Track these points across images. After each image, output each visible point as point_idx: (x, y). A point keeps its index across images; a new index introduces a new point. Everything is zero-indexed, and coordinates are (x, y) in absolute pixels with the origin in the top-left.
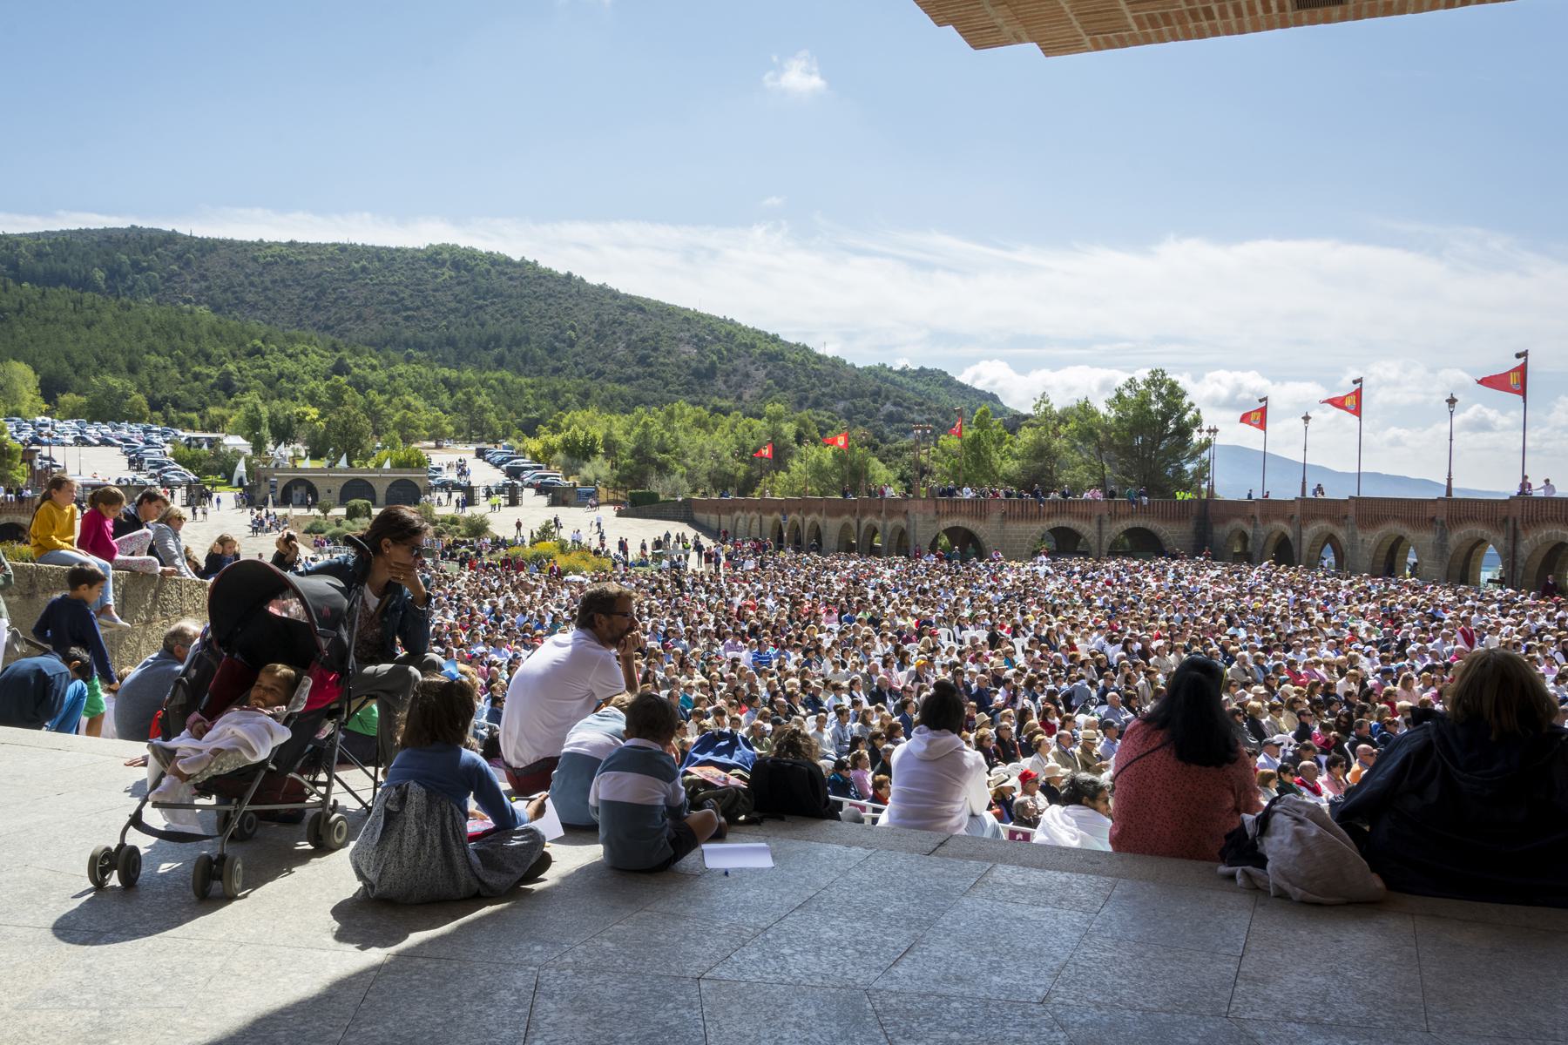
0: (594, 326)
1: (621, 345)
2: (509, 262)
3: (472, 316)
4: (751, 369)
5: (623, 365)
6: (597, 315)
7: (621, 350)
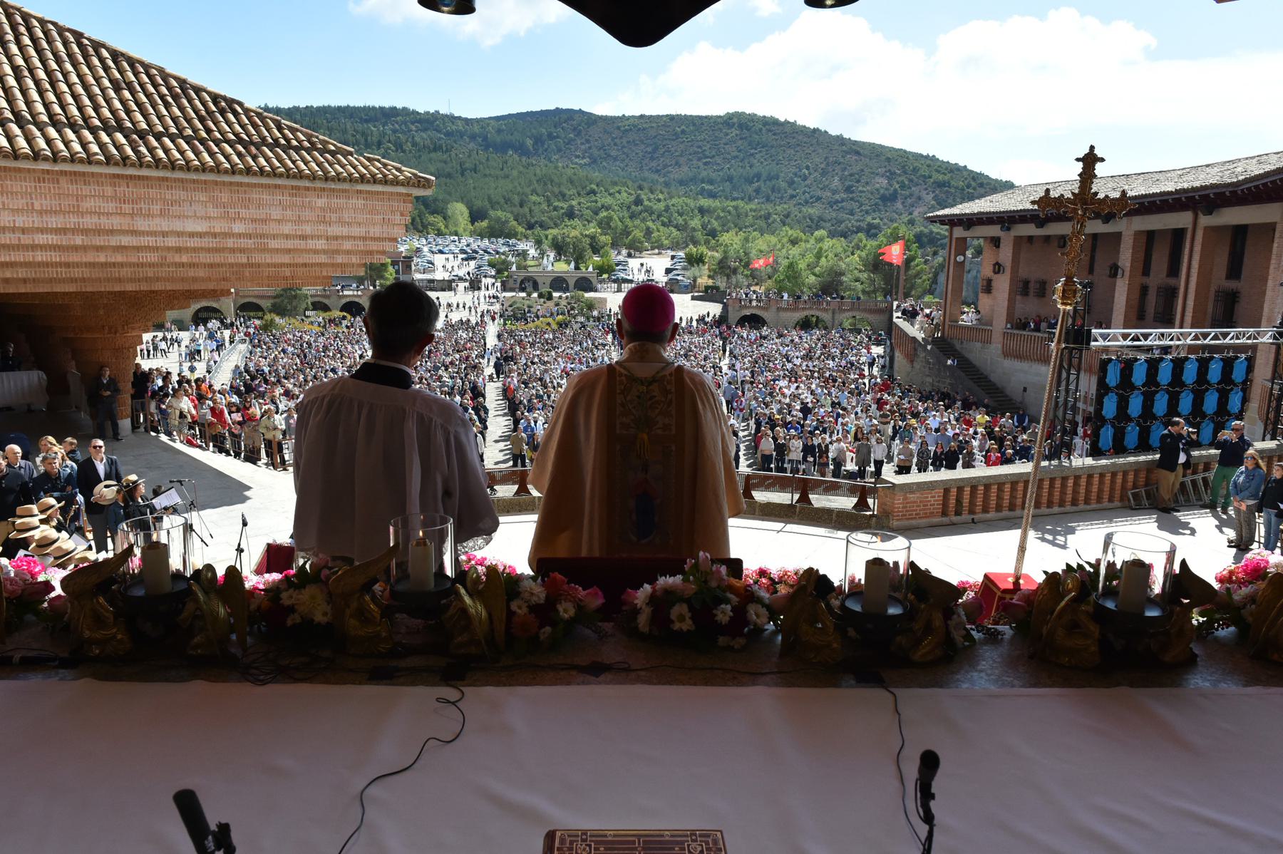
1: (837, 178)
5: (834, 192)
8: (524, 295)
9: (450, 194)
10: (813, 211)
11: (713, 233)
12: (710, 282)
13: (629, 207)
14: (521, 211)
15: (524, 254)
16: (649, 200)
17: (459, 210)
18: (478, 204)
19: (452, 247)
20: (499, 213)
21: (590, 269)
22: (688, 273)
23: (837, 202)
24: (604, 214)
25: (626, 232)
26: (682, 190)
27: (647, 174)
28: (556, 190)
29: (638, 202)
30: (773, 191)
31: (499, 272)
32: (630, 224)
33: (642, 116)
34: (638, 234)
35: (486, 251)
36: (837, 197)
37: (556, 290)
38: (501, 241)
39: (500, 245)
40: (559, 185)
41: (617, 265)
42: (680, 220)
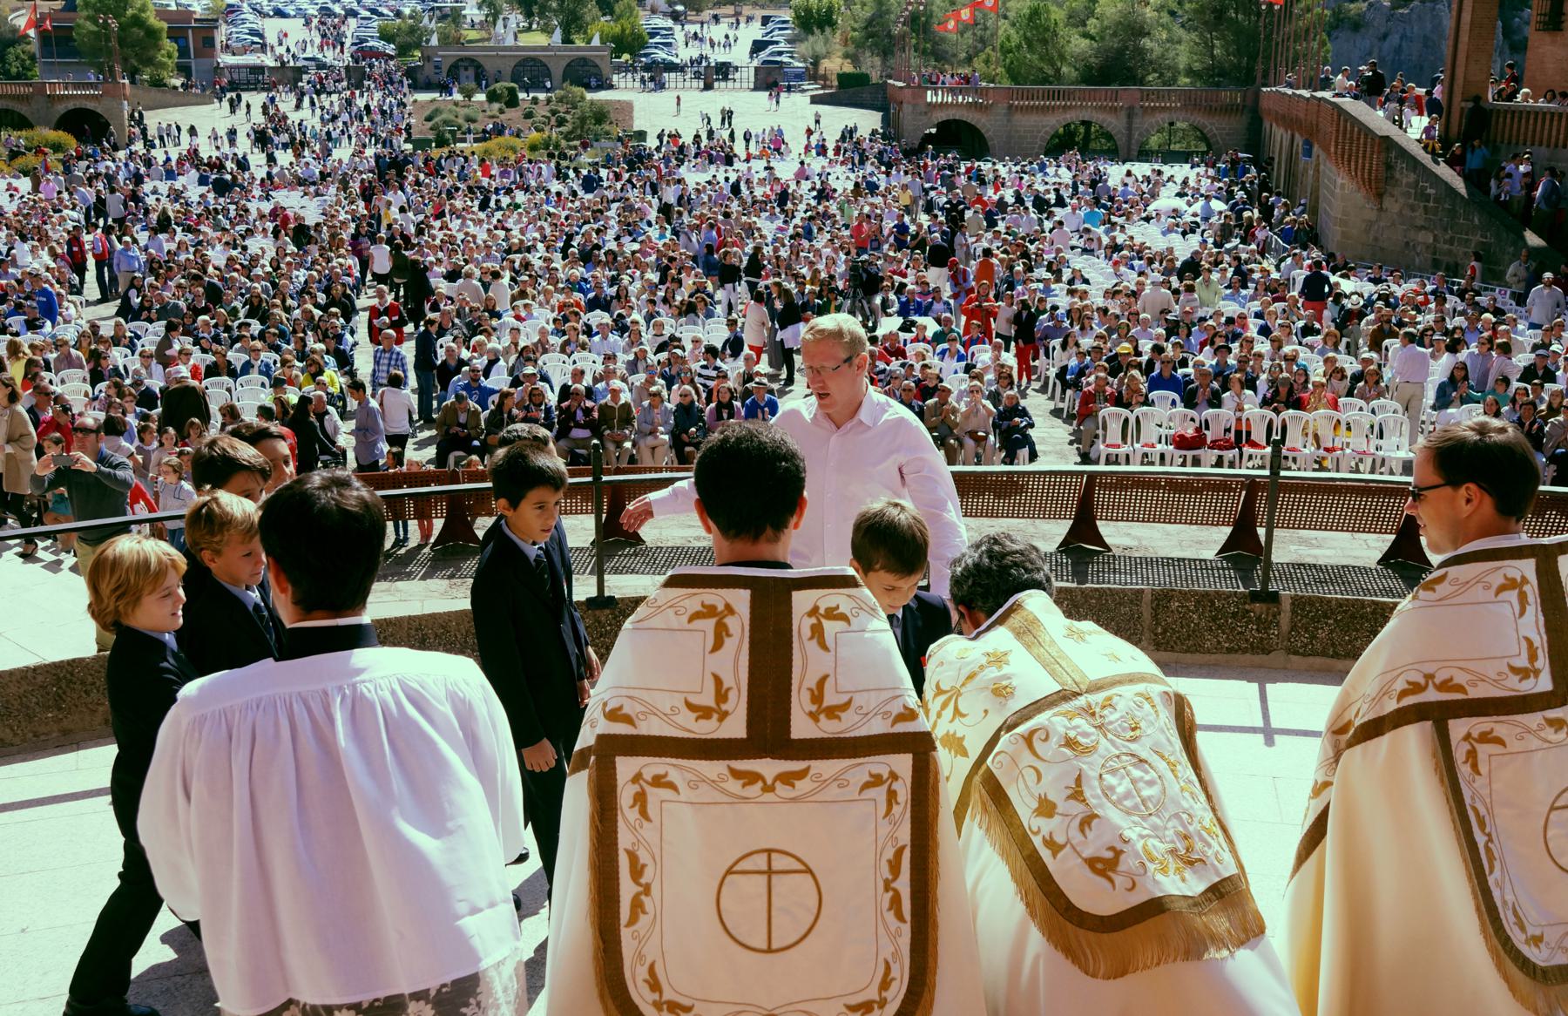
21: (596, 42)
31: (403, 50)
35: (374, 11)
41: (652, 35)
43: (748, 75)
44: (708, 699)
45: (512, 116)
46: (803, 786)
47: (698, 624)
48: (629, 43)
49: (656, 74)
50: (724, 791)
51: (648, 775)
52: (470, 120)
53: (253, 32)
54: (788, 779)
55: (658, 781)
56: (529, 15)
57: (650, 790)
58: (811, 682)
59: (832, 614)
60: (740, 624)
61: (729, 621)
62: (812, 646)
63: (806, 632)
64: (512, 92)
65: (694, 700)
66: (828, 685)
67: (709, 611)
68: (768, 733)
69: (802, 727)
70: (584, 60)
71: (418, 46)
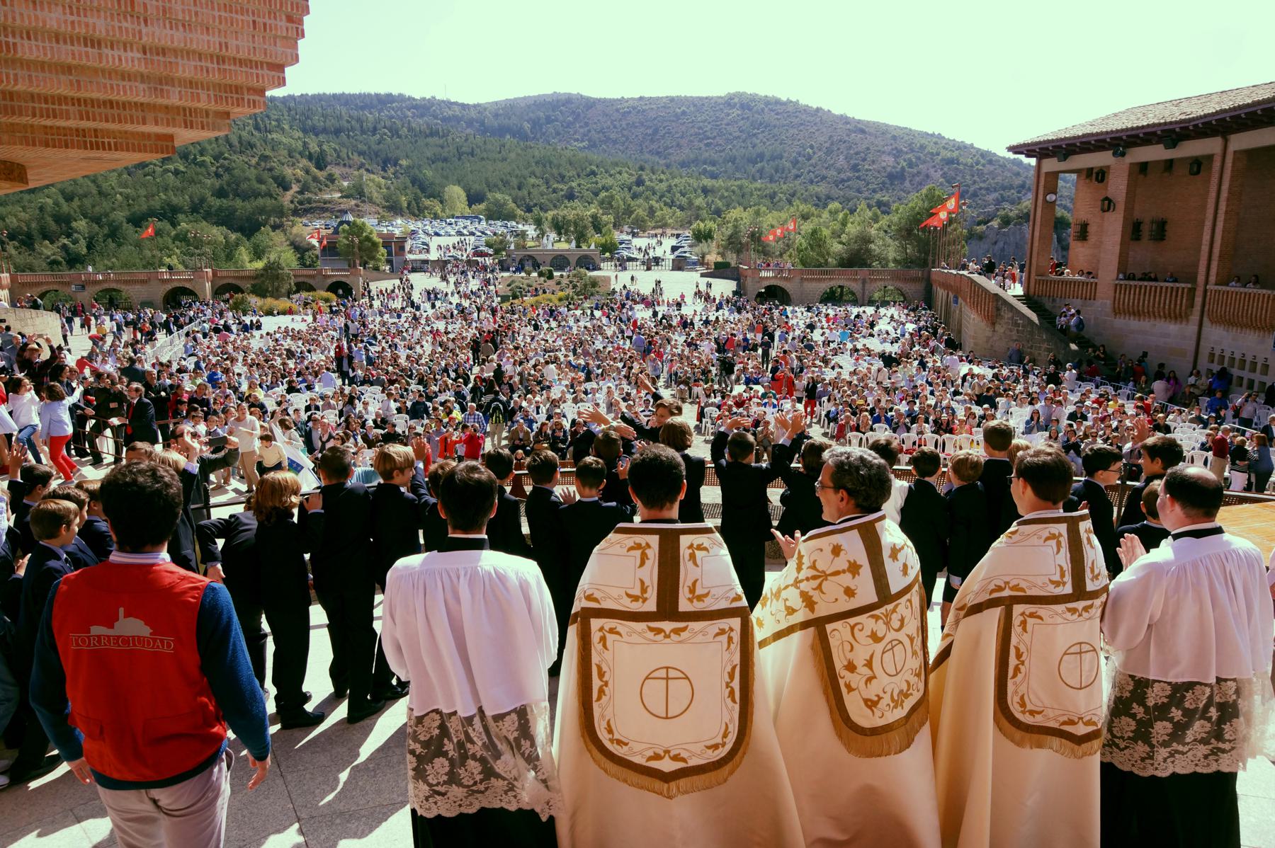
0: (827, 145)
1: (841, 157)
2: (778, 102)
3: (749, 141)
4: (932, 171)
6: (831, 137)
7: (841, 161)
8: (523, 274)
9: (447, 178)
10: (822, 189)
11: (718, 212)
12: (720, 259)
13: (630, 189)
14: (520, 194)
15: (523, 234)
16: (651, 180)
17: (456, 193)
18: (476, 187)
19: (449, 229)
20: (499, 196)
21: (593, 247)
22: (697, 249)
23: (843, 181)
24: (603, 194)
25: (629, 211)
26: (684, 171)
27: (647, 156)
28: (555, 171)
29: (640, 182)
30: (777, 171)
31: (497, 252)
32: (632, 203)
33: (641, 98)
34: (641, 212)
36: (842, 176)
37: (557, 270)
38: (499, 223)
39: (499, 227)
40: (559, 166)
42: (684, 201)
43: (669, 264)
44: (637, 592)
45: (550, 282)
46: (684, 635)
47: (632, 553)
48: (609, 248)
49: (622, 264)
50: (645, 638)
51: (607, 628)
52: (529, 286)
53: (424, 244)
54: (677, 631)
55: (612, 631)
56: (559, 234)
57: (608, 635)
58: (689, 583)
59: (700, 547)
60: (653, 553)
61: (648, 552)
62: (690, 564)
63: (687, 557)
64: (551, 272)
65: (630, 592)
66: (698, 584)
67: (638, 546)
68: (668, 608)
69: (684, 605)
70: (586, 257)
71: (504, 249)
